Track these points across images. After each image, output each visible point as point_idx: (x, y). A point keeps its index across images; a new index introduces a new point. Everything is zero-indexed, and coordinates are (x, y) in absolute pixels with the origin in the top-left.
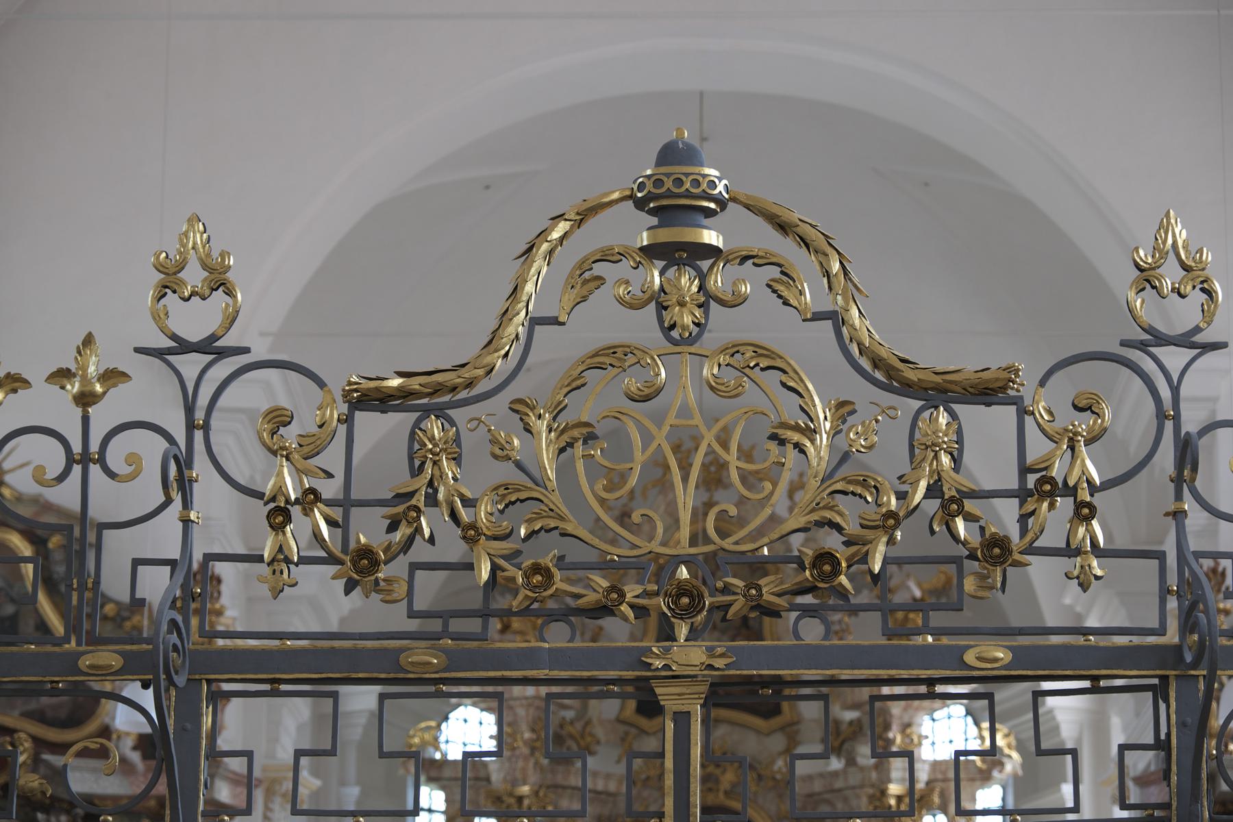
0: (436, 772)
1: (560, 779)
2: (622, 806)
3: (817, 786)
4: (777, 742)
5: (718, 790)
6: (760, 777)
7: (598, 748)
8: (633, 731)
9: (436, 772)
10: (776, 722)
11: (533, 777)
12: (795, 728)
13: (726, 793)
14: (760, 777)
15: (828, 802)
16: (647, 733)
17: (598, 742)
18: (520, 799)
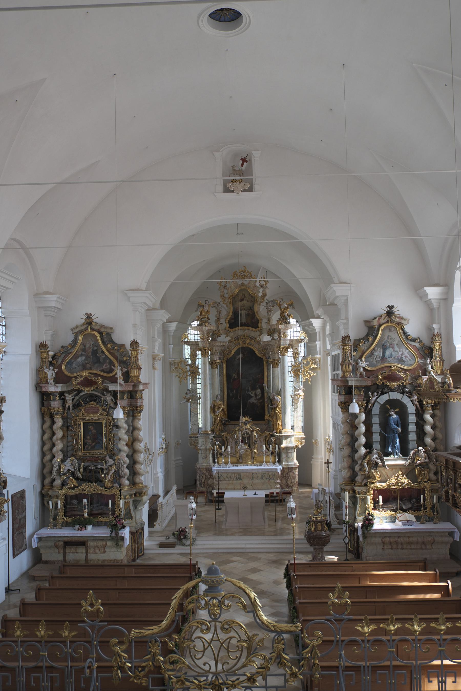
0: (188, 343)
1: (213, 344)
4: (258, 333)
6: (254, 341)
9: (188, 343)
10: (258, 329)
11: (208, 345)
14: (254, 341)
18: (205, 350)
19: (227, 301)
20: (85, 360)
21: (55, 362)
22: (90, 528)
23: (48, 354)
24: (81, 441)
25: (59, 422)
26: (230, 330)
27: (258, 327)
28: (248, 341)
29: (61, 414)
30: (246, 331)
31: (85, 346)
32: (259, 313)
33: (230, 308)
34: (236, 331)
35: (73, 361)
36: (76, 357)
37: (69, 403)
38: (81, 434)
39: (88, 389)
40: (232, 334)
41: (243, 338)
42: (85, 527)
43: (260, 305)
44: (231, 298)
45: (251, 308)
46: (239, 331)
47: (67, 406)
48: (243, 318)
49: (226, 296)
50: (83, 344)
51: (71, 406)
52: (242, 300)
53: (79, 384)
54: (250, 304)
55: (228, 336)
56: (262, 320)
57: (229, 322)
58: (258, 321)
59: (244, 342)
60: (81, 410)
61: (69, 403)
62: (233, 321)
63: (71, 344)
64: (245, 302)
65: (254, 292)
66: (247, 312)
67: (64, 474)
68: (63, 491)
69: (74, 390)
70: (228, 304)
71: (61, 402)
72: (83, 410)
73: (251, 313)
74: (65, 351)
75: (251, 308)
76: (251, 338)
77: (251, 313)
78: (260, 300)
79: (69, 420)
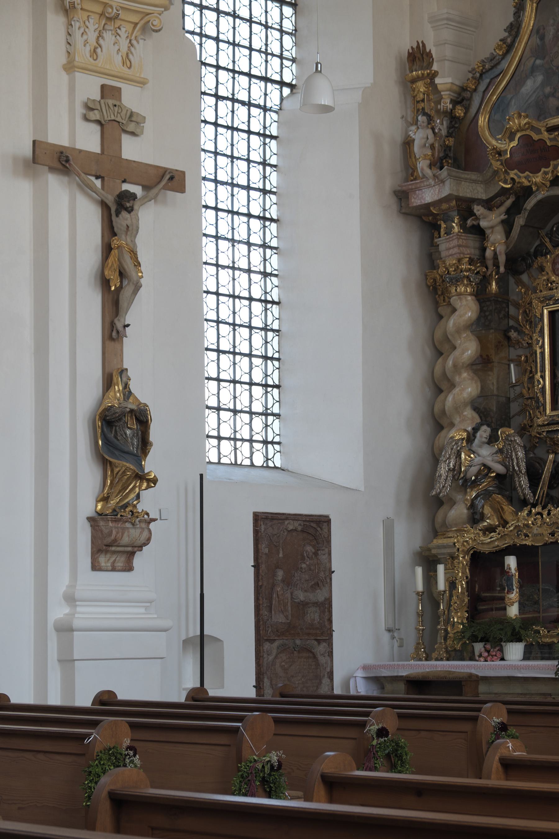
20: (543, 85)
21: (459, 112)
22: (515, 651)
23: (435, 86)
24: (543, 377)
25: (466, 309)
29: (468, 277)
31: (542, 38)
35: (509, 96)
36: (517, 80)
37: (497, 243)
38: (543, 354)
39: (538, 178)
42: (501, 650)
47: (489, 253)
50: (539, 31)
51: (501, 249)
53: (509, 165)
60: (542, 269)
61: (497, 243)
63: (503, 40)
67: (474, 484)
68: (467, 537)
69: (504, 192)
71: (472, 242)
72: (548, 267)
74: (487, 70)
79: (512, 311)
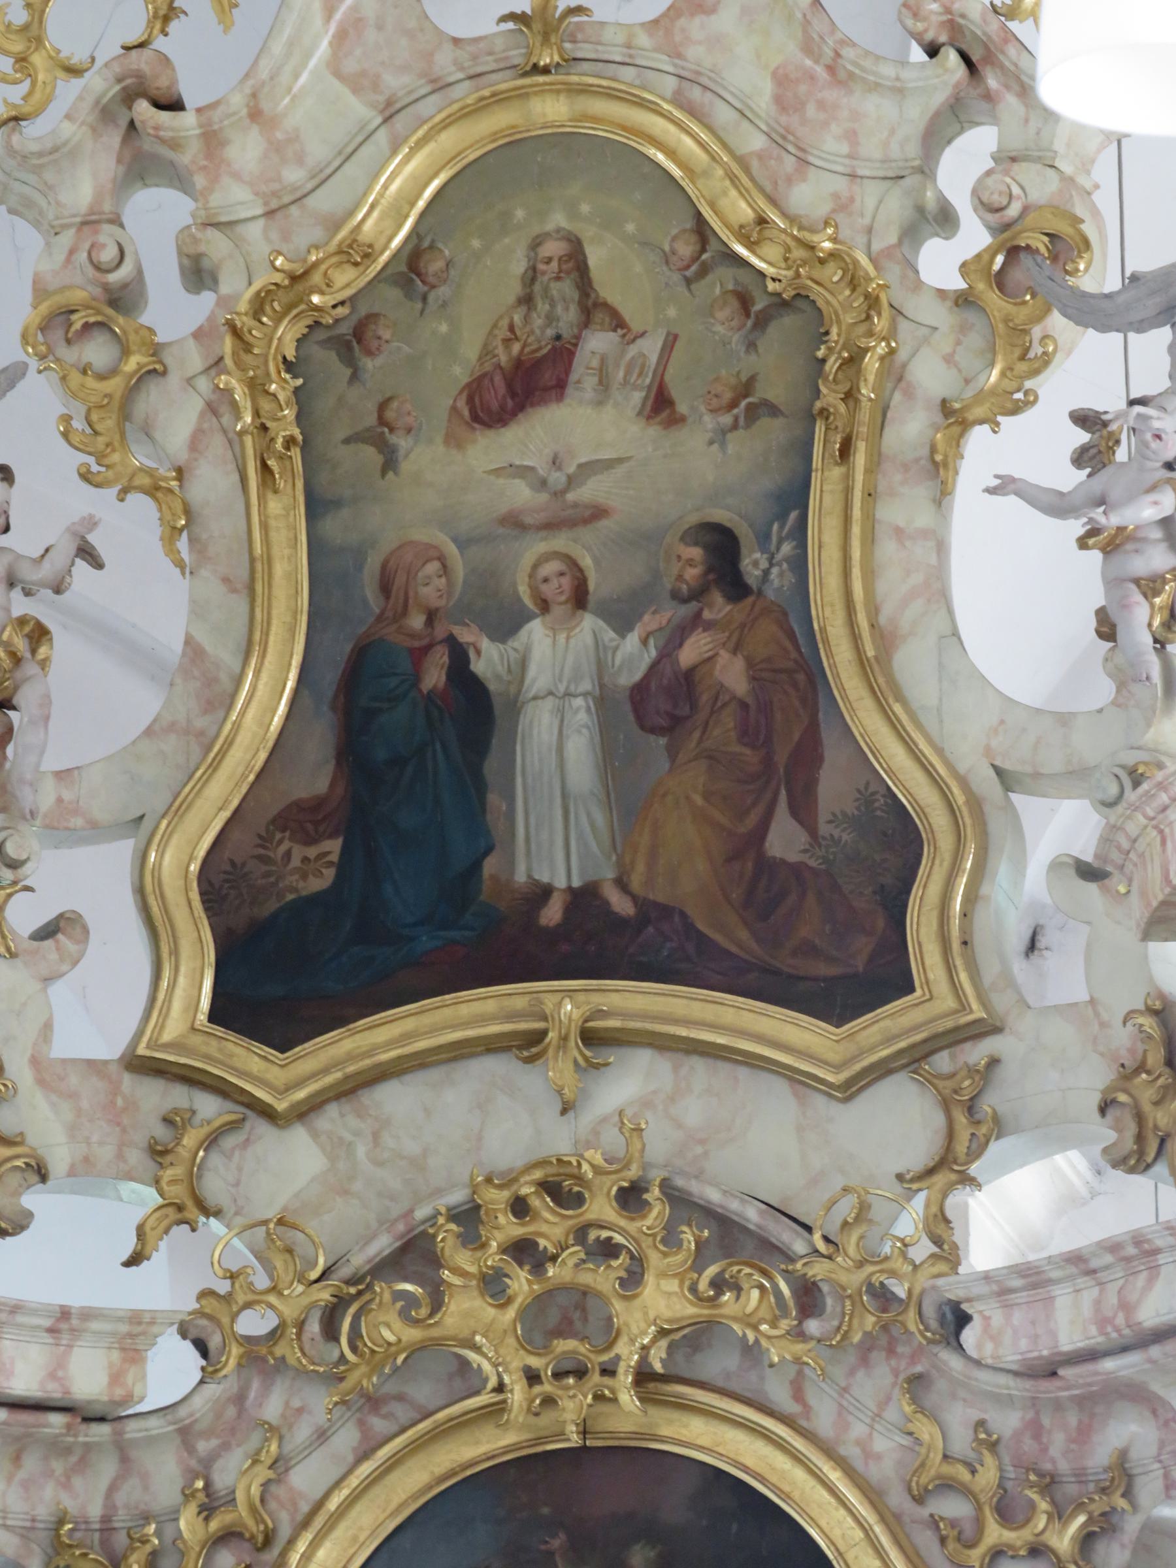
2: (164, 1476)
3: (1070, 1323)
5: (608, 1371)
6: (808, 1298)
7: (34, 1200)
8: (208, 1107)
12: (977, 1053)
13: (644, 1377)
14: (808, 1298)
15: (1136, 1394)
16: (267, 1113)
17: (42, 1174)
19: (176, 415)
26: (248, 1061)
27: (890, 978)
28: (663, 1299)
30: (628, 1082)
32: (914, 664)
33: (251, 585)
34: (393, 1098)
40: (284, 1168)
41: (550, 1225)
43: (939, 469)
44: (287, 335)
45: (721, 545)
46: (448, 1104)
48: (558, 811)
49: (173, 314)
52: (523, 383)
54: (704, 470)
55: (188, 1207)
56: (977, 824)
57: (219, 883)
58: (896, 840)
59: (563, 1316)
62: (311, 868)
64: (585, 428)
65: (809, 196)
66: (633, 654)
70: (213, 483)
73: (733, 675)
75: (721, 545)
76: (728, 1240)
77: (733, 675)
78: (931, 375)
